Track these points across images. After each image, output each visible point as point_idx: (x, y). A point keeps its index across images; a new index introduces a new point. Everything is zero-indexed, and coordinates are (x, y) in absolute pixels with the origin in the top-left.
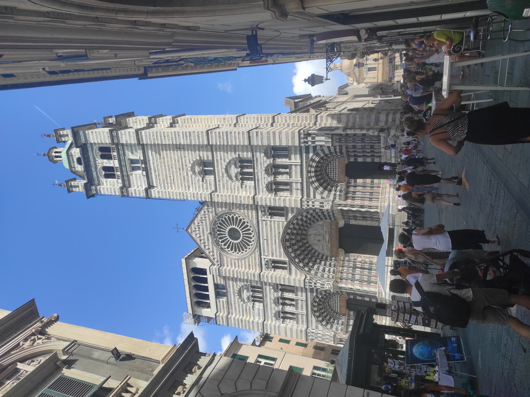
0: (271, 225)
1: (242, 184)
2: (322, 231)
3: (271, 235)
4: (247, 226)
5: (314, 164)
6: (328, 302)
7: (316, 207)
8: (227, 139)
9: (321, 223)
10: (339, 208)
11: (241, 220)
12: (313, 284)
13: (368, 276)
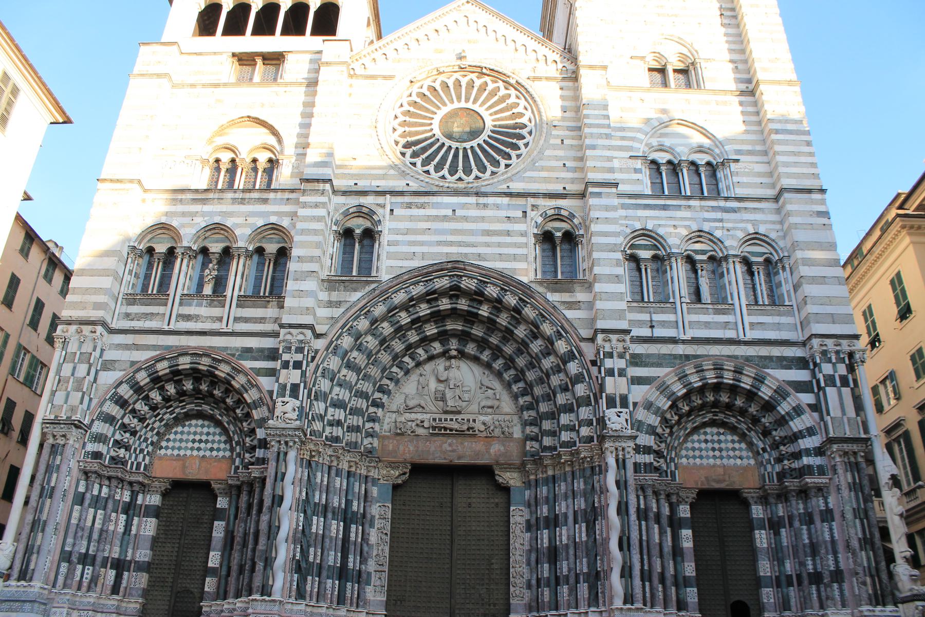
0: (508, 233)
1: (644, 157)
2: (474, 407)
3: (472, 232)
4: (496, 163)
5: (746, 383)
6: (200, 415)
7: (609, 381)
8: (791, 132)
9: (507, 405)
10: (611, 461)
11: (515, 147)
12: (299, 357)
13: (320, 566)
